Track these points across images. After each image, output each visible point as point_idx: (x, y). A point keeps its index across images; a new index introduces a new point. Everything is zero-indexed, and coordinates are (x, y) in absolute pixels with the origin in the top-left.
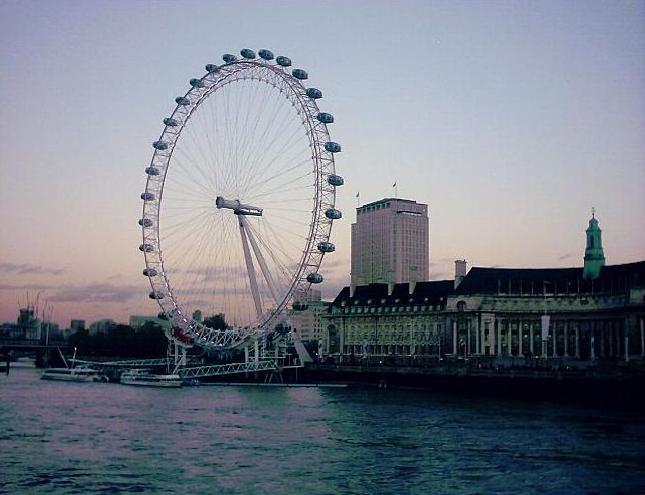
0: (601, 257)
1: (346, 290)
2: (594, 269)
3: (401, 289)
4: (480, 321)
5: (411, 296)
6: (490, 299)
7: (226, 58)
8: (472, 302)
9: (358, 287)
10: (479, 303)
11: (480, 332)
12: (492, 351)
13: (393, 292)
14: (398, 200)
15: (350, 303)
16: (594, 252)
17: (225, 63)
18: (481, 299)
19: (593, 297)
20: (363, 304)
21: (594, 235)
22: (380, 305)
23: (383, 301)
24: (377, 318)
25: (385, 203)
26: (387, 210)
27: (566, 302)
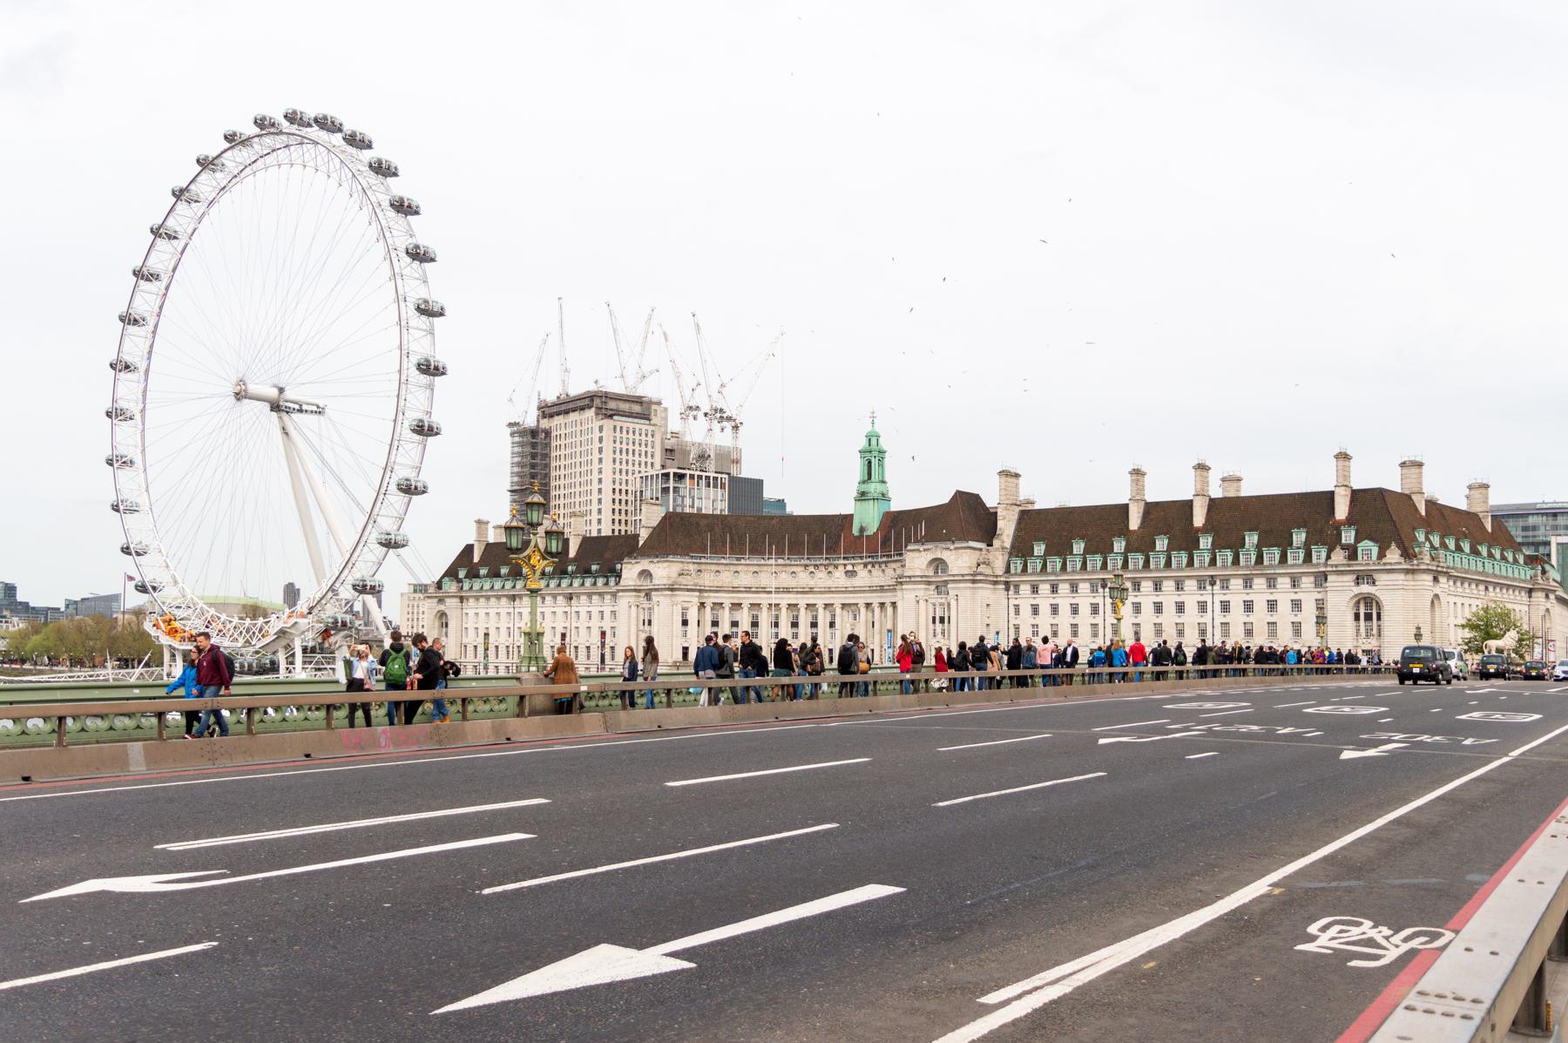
0: (884, 497)
1: (469, 549)
2: (869, 519)
5: (575, 560)
6: (691, 567)
7: (261, 123)
8: (663, 570)
9: (488, 545)
10: (674, 575)
15: (473, 574)
16: (873, 488)
17: (257, 130)
19: (865, 565)
20: (495, 574)
21: (872, 459)
24: (513, 598)
27: (821, 574)
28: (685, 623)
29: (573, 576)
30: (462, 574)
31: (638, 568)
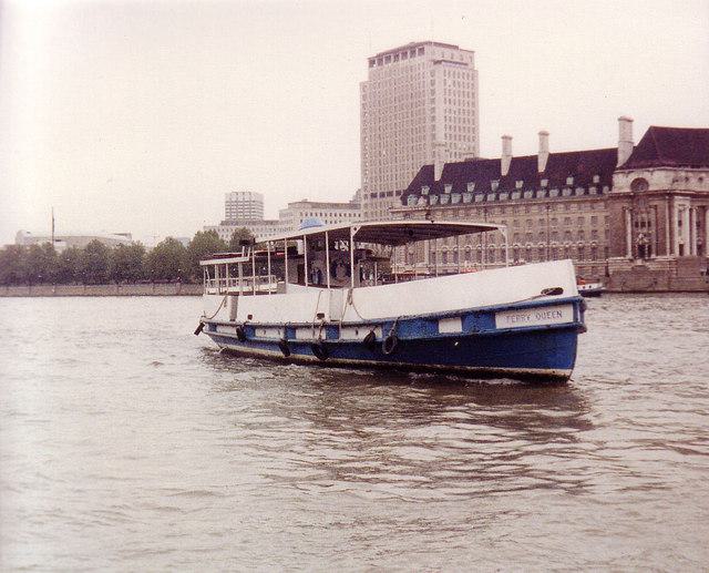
1: (428, 171)
3: (524, 166)
4: (671, 207)
5: (547, 174)
8: (659, 179)
10: (671, 179)
11: (671, 223)
12: (687, 252)
13: (511, 169)
14: (436, 44)
15: (437, 189)
18: (672, 175)
22: (488, 190)
23: (495, 184)
25: (415, 49)
26: (418, 60)
28: (680, 223)
29: (547, 189)
30: (425, 190)
31: (633, 177)
